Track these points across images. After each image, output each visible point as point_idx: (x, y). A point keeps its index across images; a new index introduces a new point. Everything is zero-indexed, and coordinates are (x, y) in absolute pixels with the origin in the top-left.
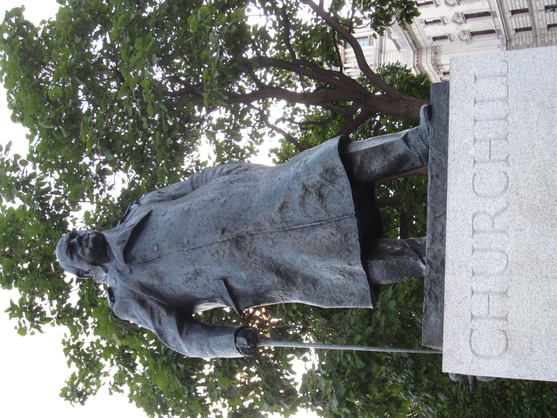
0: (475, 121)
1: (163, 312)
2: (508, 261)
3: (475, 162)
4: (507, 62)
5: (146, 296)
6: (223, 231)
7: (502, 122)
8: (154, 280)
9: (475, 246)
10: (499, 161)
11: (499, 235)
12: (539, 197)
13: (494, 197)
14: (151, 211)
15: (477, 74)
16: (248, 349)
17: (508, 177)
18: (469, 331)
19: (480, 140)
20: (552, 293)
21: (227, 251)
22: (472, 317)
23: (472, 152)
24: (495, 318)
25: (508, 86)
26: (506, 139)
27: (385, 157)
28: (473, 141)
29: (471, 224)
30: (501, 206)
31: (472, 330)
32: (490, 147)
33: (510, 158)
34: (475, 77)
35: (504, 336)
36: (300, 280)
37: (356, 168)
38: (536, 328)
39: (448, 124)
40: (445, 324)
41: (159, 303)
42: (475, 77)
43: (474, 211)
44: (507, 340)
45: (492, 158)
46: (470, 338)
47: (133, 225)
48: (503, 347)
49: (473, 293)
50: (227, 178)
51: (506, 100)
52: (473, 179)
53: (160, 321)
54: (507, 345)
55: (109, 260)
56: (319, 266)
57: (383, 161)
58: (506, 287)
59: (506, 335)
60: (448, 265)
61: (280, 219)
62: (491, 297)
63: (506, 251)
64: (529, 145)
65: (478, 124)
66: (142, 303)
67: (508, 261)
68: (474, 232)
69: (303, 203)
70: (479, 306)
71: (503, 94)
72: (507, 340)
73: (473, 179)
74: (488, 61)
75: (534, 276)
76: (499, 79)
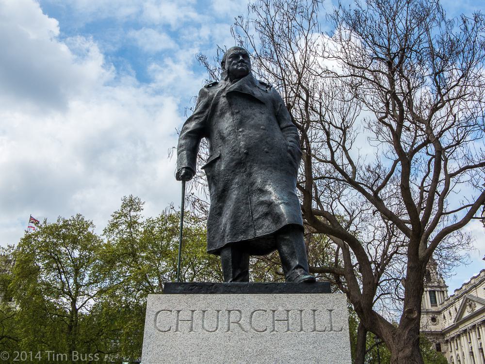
0: (301, 311)
1: (202, 119)
2: (211, 332)
3: (274, 311)
4: (341, 331)
5: (210, 107)
6: (247, 154)
7: (299, 328)
8: (219, 112)
9: (220, 312)
10: (274, 326)
11: (227, 327)
12: (250, 350)
14: (265, 104)
15: (333, 311)
16: (179, 176)
17: (263, 331)
18: (170, 309)
19: (288, 314)
20: (191, 358)
21: (235, 157)
22: (179, 311)
23: (280, 308)
24: (177, 324)
25: (325, 331)
26: (288, 330)
27: (289, 254)
28: (288, 309)
29: (234, 309)
30: (244, 327)
31: (171, 311)
32: (283, 320)
33: (275, 332)
34: (332, 310)
35: (167, 330)
36: (220, 205)
37: (283, 236)
38: (171, 348)
39: (301, 293)
40: (175, 295)
41: (207, 117)
42: (332, 310)
43: (242, 311)
44: (165, 332)
45: (276, 322)
46: (167, 310)
47: (253, 93)
48: (161, 329)
49: (193, 311)
52: (262, 310)
53: (197, 118)
54: (162, 332)
55: (231, 81)
56: (227, 216)
57: (286, 253)
58: (196, 331)
59: (168, 331)
60: (210, 296)
61: (254, 189)
62: (190, 322)
63: (217, 331)
64: (284, 345)
65: (299, 312)
66: (206, 106)
67: (211, 332)
68: (229, 311)
69: (262, 203)
71: (318, 328)
72: (165, 332)
73: (262, 310)
74: (342, 318)
75: (201, 347)
76: (330, 325)
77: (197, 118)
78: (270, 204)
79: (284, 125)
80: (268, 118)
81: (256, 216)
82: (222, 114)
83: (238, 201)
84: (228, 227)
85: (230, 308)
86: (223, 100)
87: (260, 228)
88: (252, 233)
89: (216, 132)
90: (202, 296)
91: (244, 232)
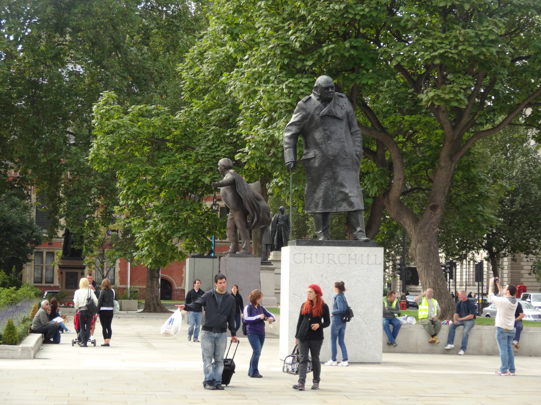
13: (339, 260)
23: (353, 254)
41: (305, 125)
50: (354, 156)
51: (368, 264)
55: (322, 102)
60: (319, 247)
69: (342, 192)
70: (308, 256)
71: (370, 263)
77: (298, 125)
78: (346, 194)
79: (353, 130)
80: (345, 132)
81: (338, 199)
82: (317, 127)
83: (327, 188)
84: (321, 202)
85: (329, 253)
86: (317, 118)
87: (340, 206)
88: (335, 208)
89: (310, 137)
90: (315, 247)
91: (331, 207)
